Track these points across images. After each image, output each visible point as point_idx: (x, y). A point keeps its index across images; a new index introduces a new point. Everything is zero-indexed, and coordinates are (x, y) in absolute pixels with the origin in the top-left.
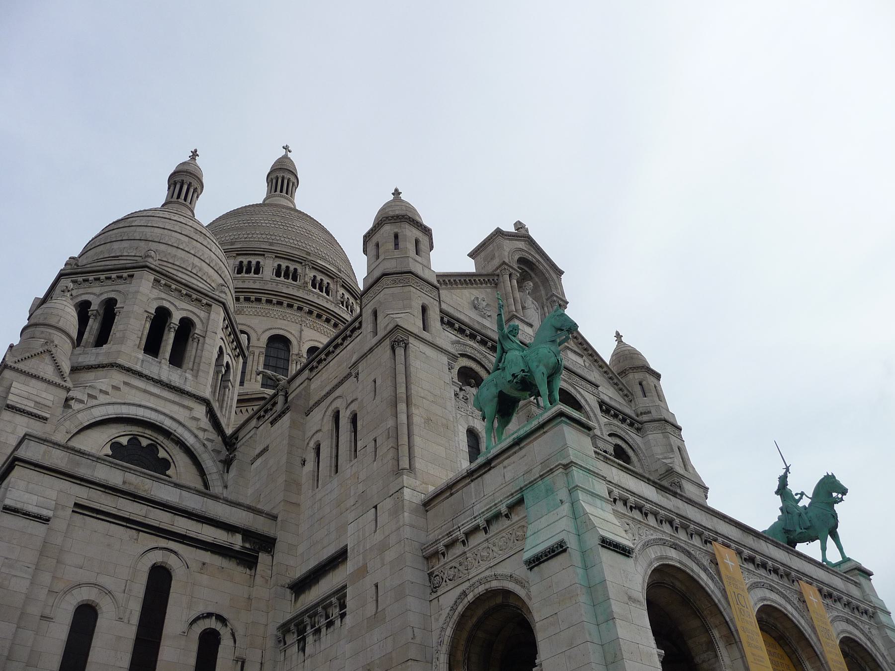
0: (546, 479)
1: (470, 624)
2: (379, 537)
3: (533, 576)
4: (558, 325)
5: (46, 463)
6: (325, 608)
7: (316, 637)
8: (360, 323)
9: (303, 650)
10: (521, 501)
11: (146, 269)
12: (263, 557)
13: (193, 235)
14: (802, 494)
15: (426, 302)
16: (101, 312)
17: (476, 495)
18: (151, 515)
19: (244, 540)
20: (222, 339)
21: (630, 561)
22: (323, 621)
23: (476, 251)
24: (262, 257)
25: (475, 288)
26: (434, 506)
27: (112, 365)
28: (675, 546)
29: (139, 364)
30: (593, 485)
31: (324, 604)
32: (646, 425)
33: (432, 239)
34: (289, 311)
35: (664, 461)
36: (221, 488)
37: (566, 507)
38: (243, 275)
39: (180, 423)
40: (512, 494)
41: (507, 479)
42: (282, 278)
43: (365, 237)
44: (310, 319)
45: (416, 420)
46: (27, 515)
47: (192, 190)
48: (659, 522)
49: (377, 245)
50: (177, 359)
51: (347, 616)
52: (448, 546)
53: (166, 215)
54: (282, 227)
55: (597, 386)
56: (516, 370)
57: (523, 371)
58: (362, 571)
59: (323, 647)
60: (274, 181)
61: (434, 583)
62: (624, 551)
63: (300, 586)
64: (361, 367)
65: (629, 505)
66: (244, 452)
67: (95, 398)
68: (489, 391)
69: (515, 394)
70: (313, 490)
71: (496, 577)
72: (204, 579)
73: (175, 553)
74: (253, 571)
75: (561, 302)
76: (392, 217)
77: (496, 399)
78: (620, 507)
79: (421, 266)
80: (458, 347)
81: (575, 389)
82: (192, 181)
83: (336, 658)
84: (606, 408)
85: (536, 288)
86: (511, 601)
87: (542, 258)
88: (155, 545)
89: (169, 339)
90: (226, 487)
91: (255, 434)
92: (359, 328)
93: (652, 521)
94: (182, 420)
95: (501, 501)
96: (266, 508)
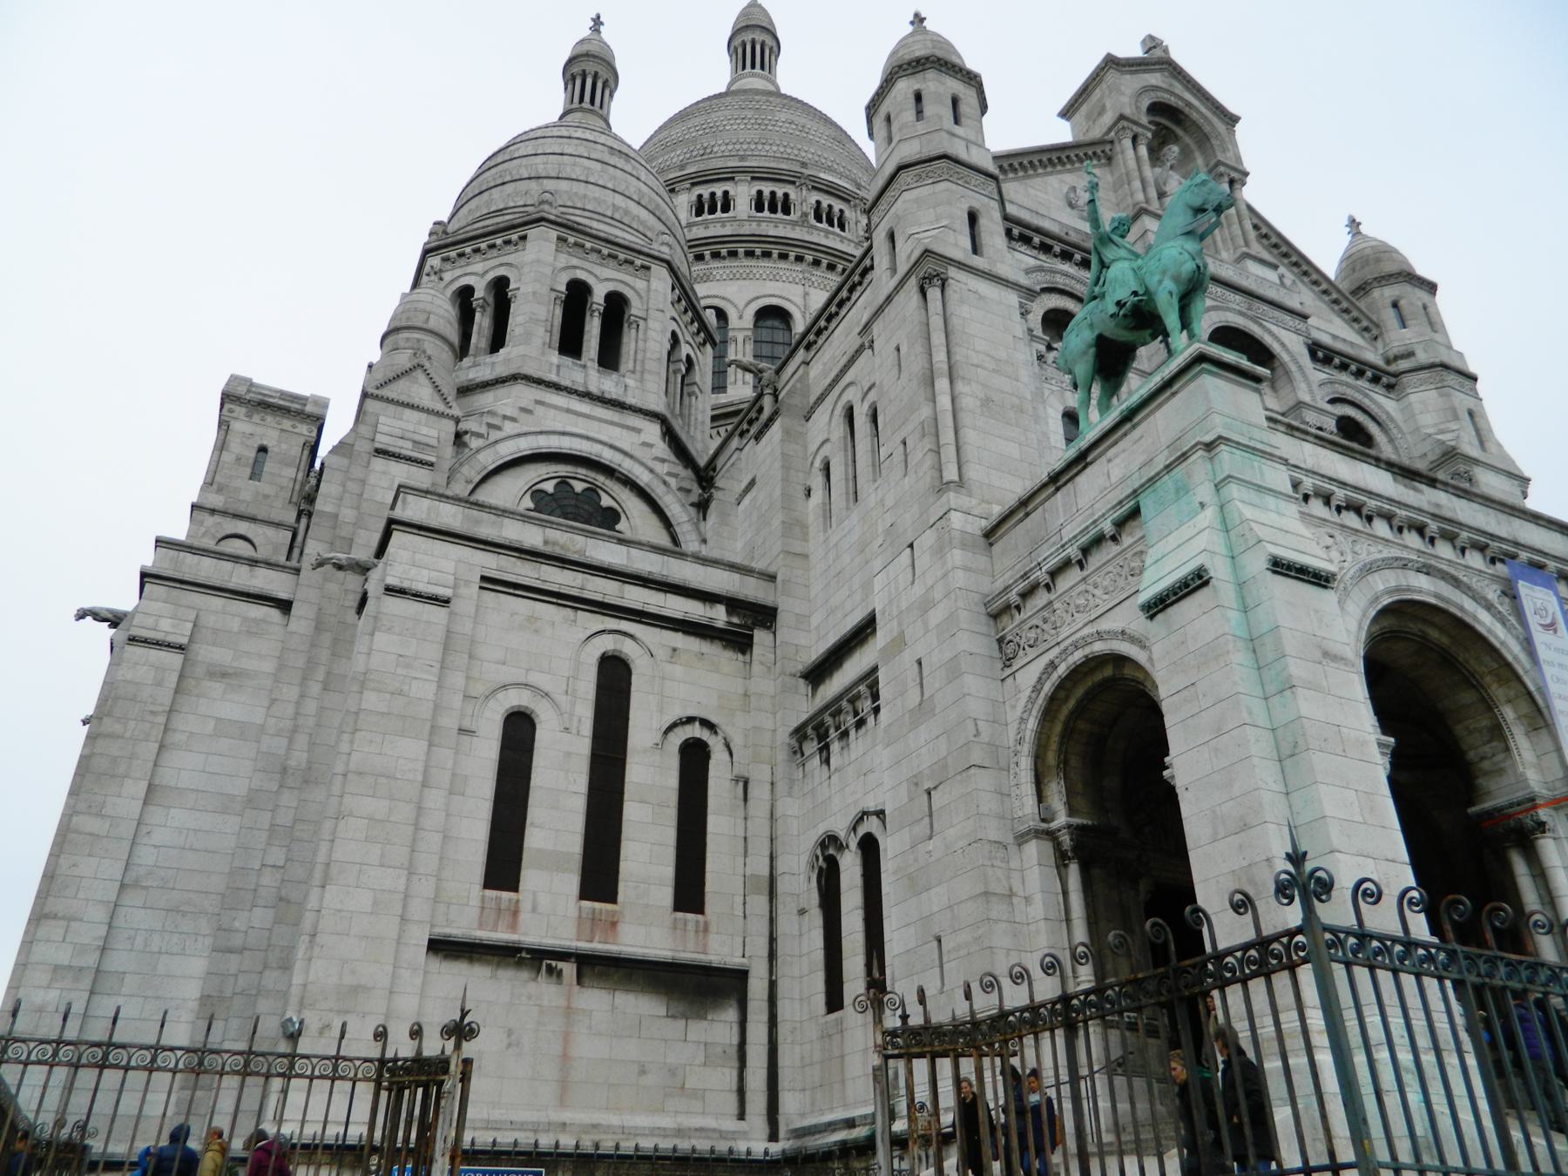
0: (1176, 471)
2: (918, 590)
4: (1197, 202)
5: (434, 524)
6: (852, 701)
7: (844, 743)
9: (827, 761)
10: (1135, 513)
12: (760, 637)
13: (607, 157)
15: (976, 205)
16: (491, 300)
17: (1065, 511)
18: (589, 586)
19: (729, 613)
20: (674, 319)
22: (850, 720)
23: (1072, 105)
25: (1069, 171)
26: (1002, 536)
27: (514, 378)
28: (1427, 570)
29: (554, 370)
30: (1262, 474)
31: (849, 696)
32: (1405, 379)
33: (983, 92)
34: (782, 265)
35: (1440, 437)
36: (697, 544)
37: (1210, 514)
38: (706, 216)
39: (626, 454)
40: (1121, 502)
41: (1114, 479)
42: (766, 213)
43: (868, 108)
45: (967, 402)
46: (418, 596)
47: (599, 85)
48: (1395, 529)
49: (888, 119)
50: (609, 358)
51: (882, 711)
52: (1026, 595)
53: (564, 132)
55: (1305, 317)
56: (1123, 294)
57: (1135, 293)
58: (899, 643)
59: (853, 757)
60: (740, 51)
61: (1006, 653)
62: (1320, 579)
63: (817, 674)
64: (876, 329)
65: (1334, 503)
66: (729, 483)
68: (1079, 338)
69: (1124, 336)
70: (825, 531)
71: (1100, 636)
72: (678, 670)
73: (631, 636)
74: (748, 657)
75: (1234, 175)
76: (909, 64)
77: (1092, 351)
78: (1317, 507)
80: (1039, 276)
81: (1261, 325)
82: (599, 69)
83: (872, 771)
84: (1321, 354)
85: (1186, 154)
86: (1128, 672)
87: (1198, 98)
88: (601, 627)
89: (593, 329)
90: (704, 541)
93: (1381, 528)
95: (1103, 515)
96: (758, 565)
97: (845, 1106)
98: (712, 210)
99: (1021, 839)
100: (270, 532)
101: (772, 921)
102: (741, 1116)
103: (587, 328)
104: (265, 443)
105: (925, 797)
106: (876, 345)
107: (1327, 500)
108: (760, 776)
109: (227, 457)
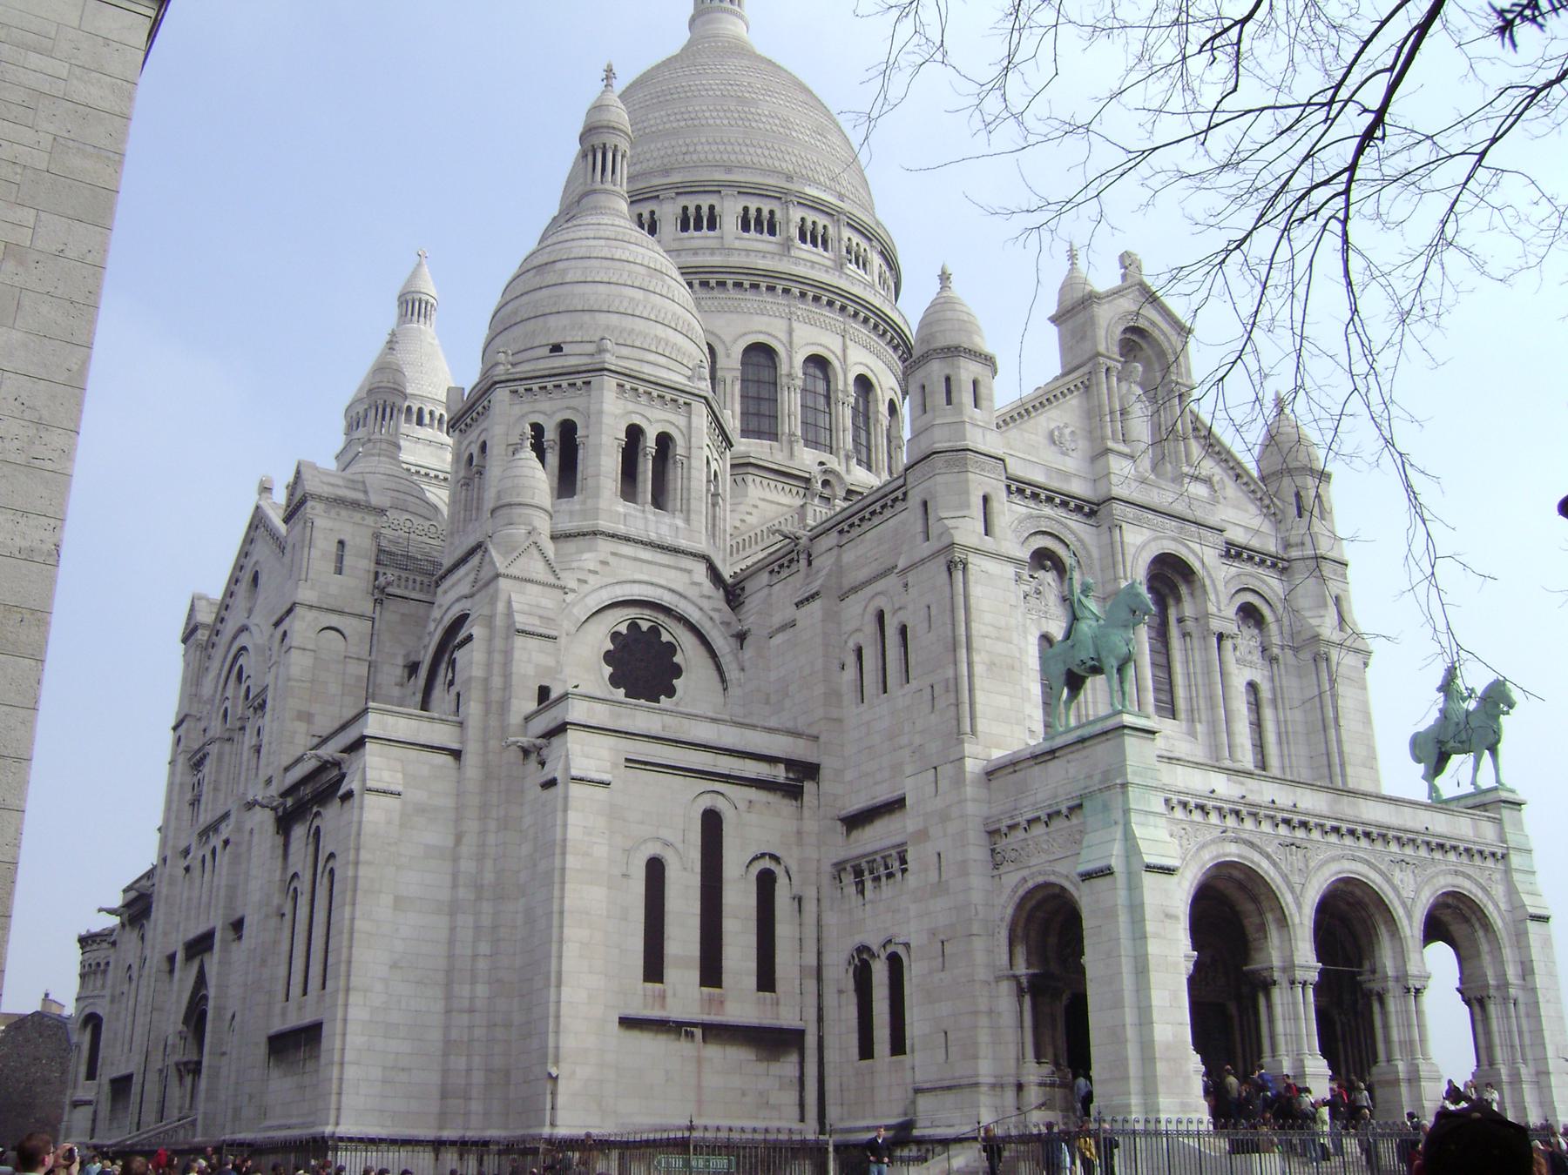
1: (1029, 906)
3: (1085, 887)
6: (884, 858)
7: (876, 884)
8: (905, 494)
9: (863, 895)
10: (1080, 806)
11: (606, 373)
12: (809, 786)
14: (1472, 690)
15: (988, 490)
16: (557, 439)
19: (787, 770)
21: (1173, 879)
24: (716, 196)
26: (997, 778)
28: (1236, 841)
29: (622, 522)
32: (1295, 564)
34: (768, 297)
35: (1311, 621)
36: (737, 672)
38: (692, 232)
39: (681, 595)
44: (802, 308)
45: (978, 669)
47: (619, 158)
50: (659, 501)
52: (1012, 827)
54: (740, 123)
57: (1092, 659)
58: (922, 835)
61: (997, 860)
62: (1168, 871)
63: (855, 821)
67: (585, 582)
69: (1086, 675)
71: (1054, 873)
74: (799, 802)
76: (942, 349)
77: (1064, 676)
78: (1179, 813)
79: (980, 430)
84: (1234, 552)
91: (770, 595)
92: (903, 500)
93: (1214, 818)
94: (680, 589)
97: (874, 1117)
98: (698, 227)
99: (998, 979)
100: (355, 622)
101: (820, 996)
102: (802, 1119)
103: (641, 468)
104: (342, 537)
105: (940, 944)
106: (910, 591)
107: (1185, 805)
108: (810, 894)
109: (315, 553)
